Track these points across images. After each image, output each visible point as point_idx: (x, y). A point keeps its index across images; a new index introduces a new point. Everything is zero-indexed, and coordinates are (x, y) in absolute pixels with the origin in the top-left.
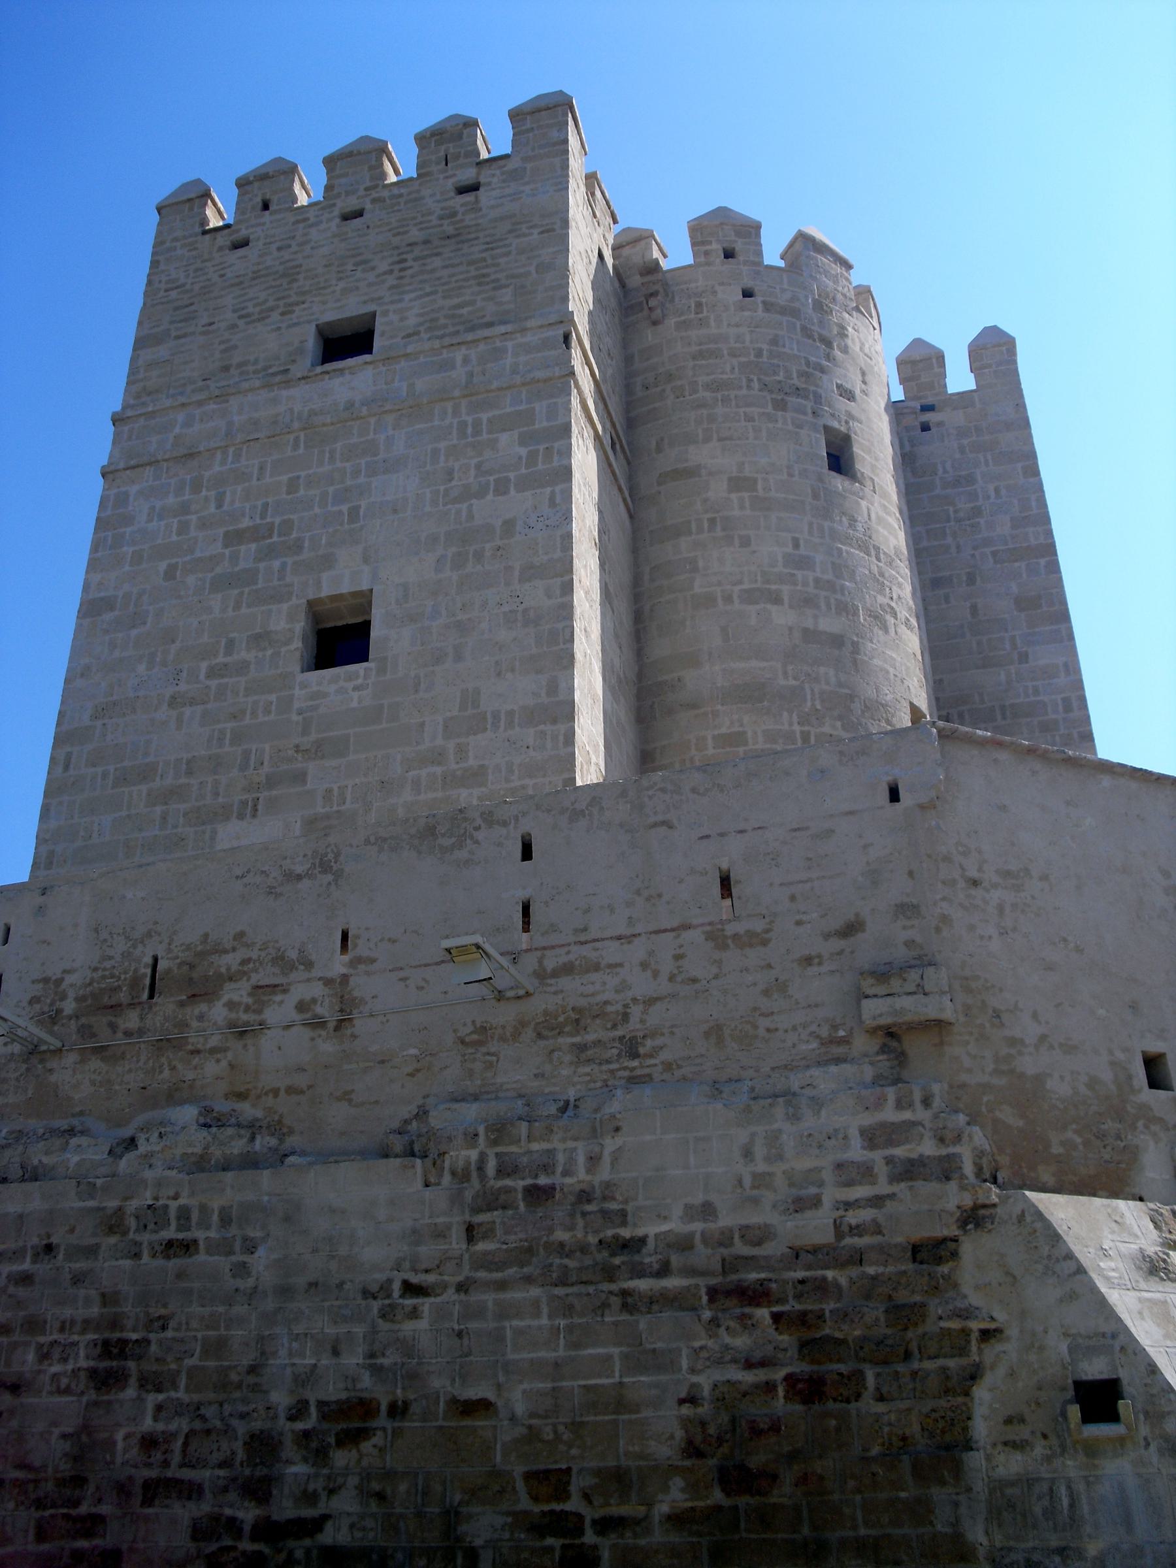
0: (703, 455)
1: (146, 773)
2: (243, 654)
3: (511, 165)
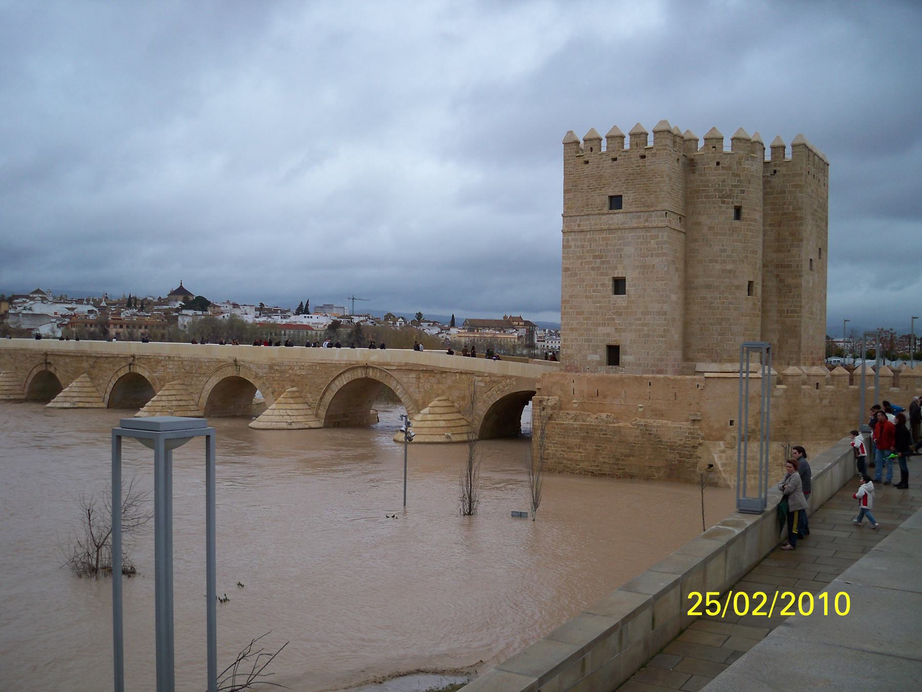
0: (703, 219)
1: (582, 313)
2: (600, 288)
3: (654, 151)
